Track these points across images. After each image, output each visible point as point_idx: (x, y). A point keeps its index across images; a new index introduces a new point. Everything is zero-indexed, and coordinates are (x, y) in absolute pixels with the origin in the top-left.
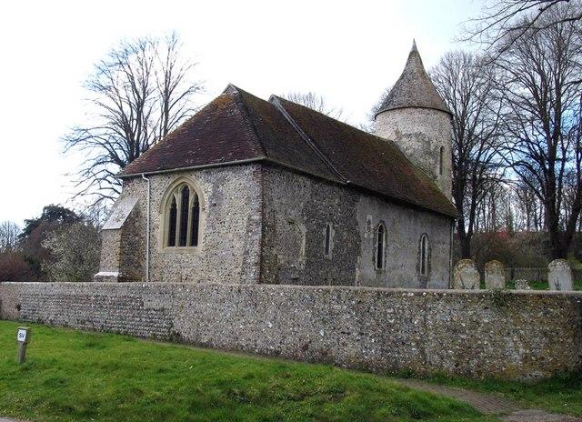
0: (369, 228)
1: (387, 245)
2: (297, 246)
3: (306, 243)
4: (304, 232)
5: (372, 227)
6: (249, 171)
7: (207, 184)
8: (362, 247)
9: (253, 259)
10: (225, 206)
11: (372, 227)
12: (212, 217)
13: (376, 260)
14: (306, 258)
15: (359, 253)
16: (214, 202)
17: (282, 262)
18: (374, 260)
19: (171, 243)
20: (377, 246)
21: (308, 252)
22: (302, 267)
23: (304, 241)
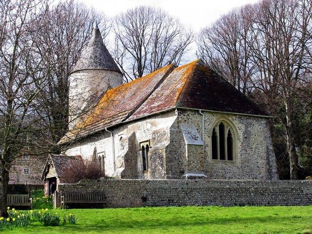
6: (263, 122)
7: (240, 125)
9: (274, 170)
10: (252, 139)
12: (244, 144)
16: (246, 136)
19: (214, 156)
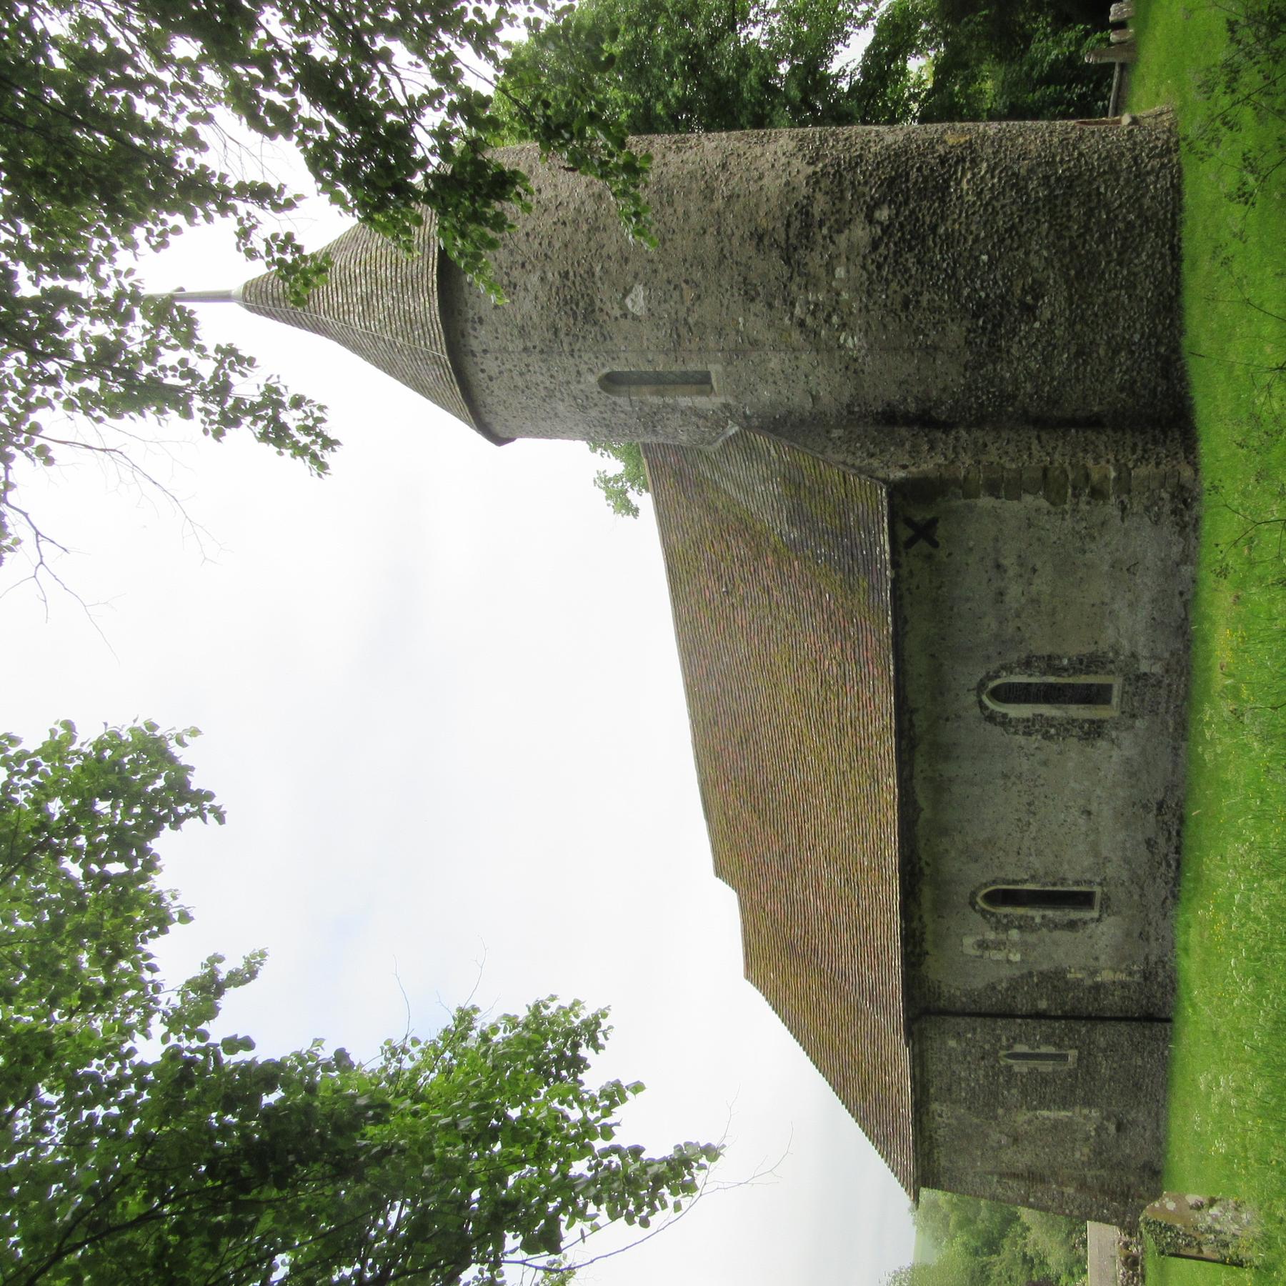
0: (999, 945)
1: (1033, 878)
2: (1056, 1126)
3: (1049, 1109)
4: (1030, 1115)
5: (991, 936)
8: (1045, 967)
11: (991, 936)
13: (1074, 915)
14: (1077, 1109)
15: (1059, 974)
17: (1086, 1150)
18: (1072, 925)
20: (1036, 914)
21: (1064, 1104)
22: (1095, 1113)
23: (1045, 1113)
